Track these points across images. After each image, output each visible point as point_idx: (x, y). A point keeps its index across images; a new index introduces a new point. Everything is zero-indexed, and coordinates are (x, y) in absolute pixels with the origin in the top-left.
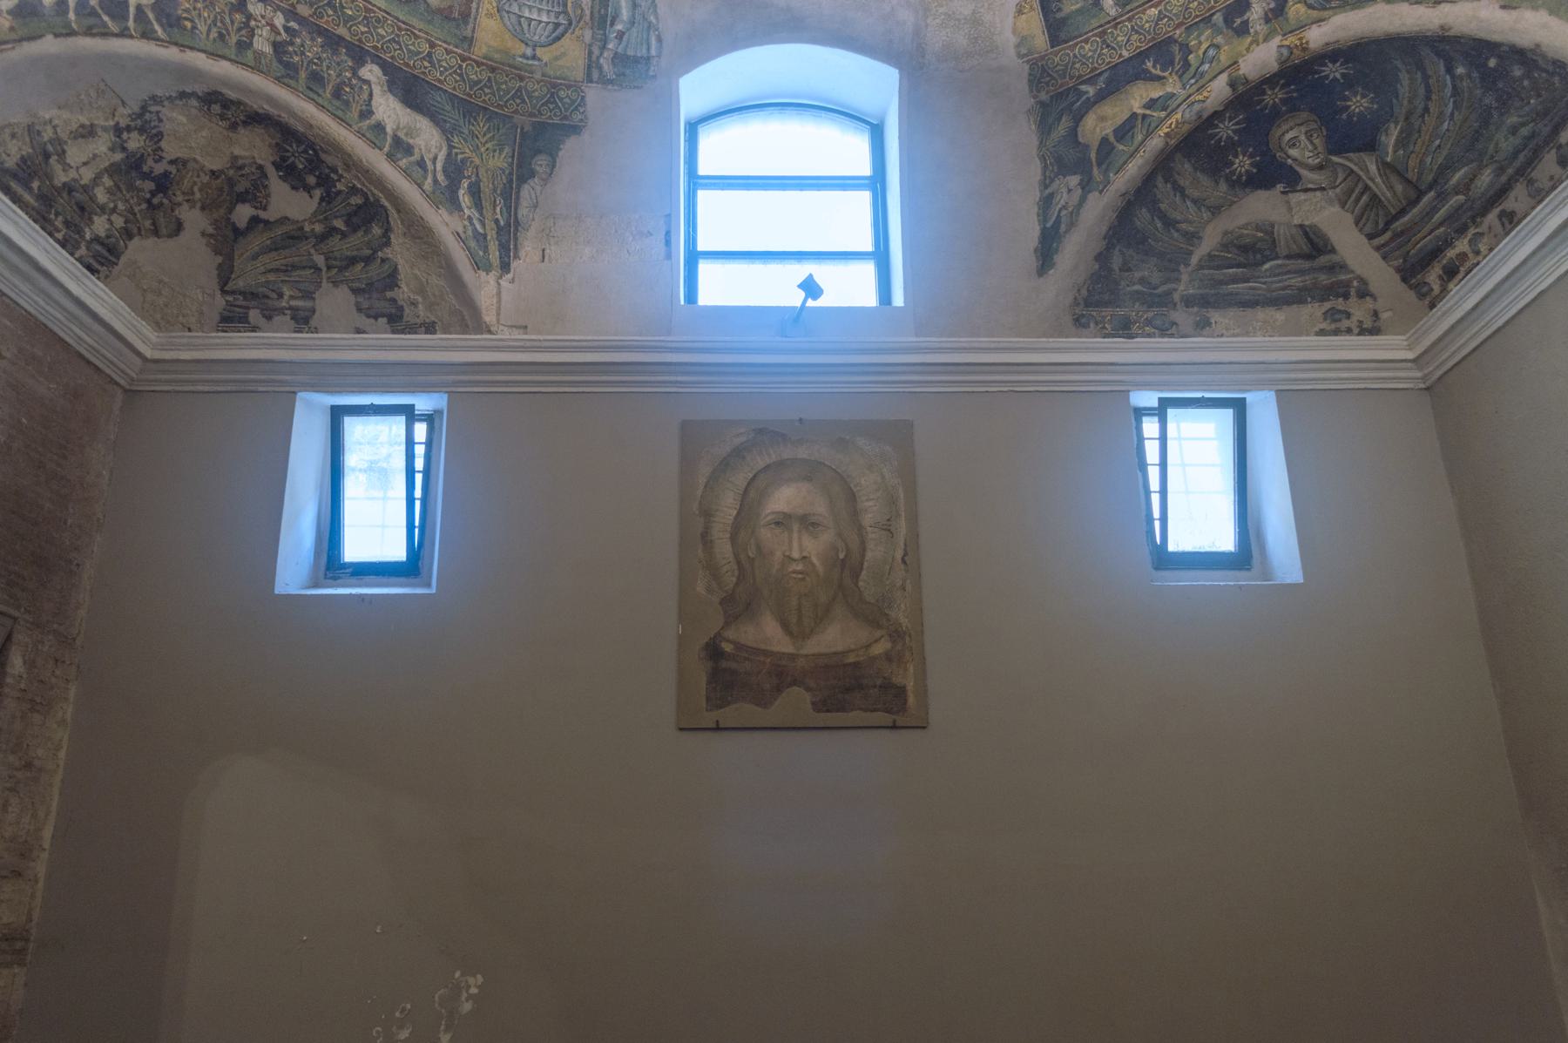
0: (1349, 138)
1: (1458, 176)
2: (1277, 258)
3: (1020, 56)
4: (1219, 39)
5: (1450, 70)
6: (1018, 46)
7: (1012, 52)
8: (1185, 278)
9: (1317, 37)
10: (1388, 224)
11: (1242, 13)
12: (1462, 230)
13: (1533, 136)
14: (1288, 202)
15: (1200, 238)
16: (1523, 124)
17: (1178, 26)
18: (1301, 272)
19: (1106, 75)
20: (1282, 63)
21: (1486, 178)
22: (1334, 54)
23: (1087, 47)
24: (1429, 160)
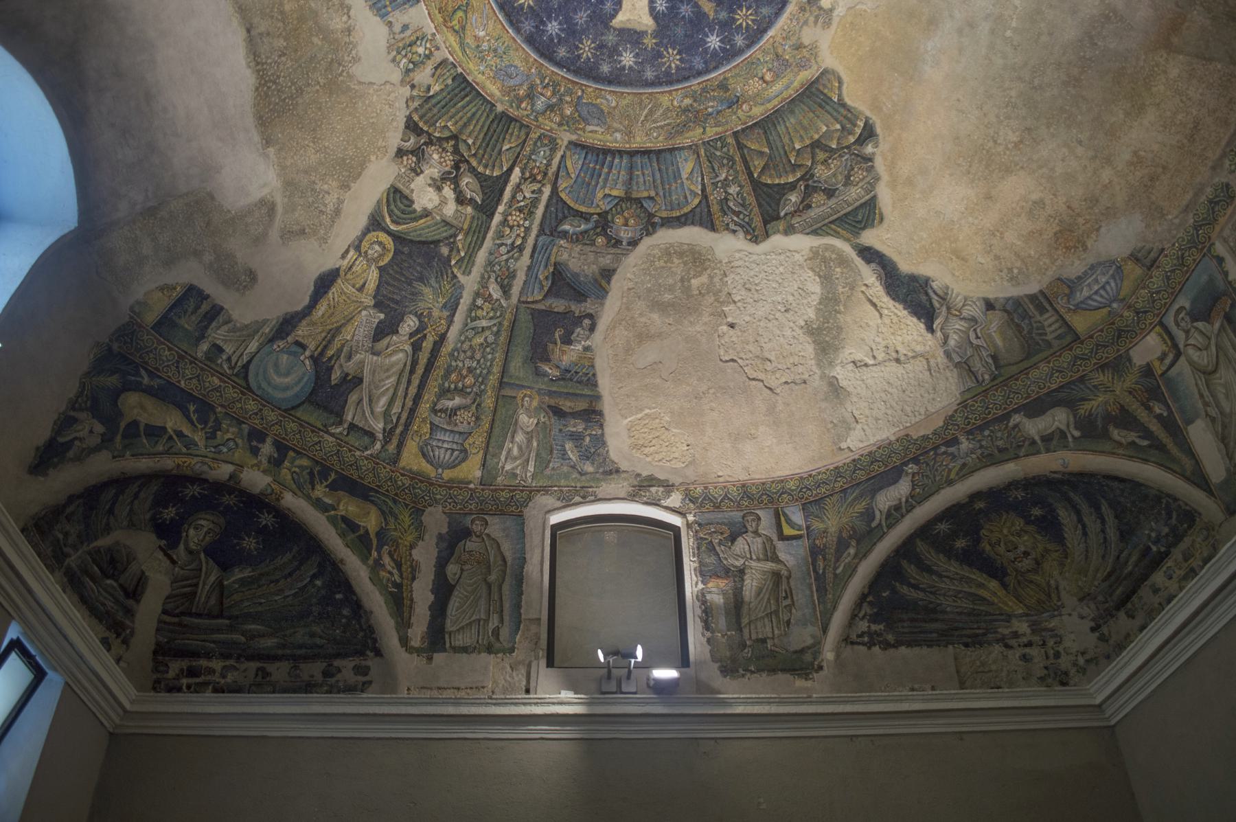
4: (239, 441)
5: (314, 577)
9: (290, 500)
11: (259, 442)
13: (321, 647)
20: (261, 493)
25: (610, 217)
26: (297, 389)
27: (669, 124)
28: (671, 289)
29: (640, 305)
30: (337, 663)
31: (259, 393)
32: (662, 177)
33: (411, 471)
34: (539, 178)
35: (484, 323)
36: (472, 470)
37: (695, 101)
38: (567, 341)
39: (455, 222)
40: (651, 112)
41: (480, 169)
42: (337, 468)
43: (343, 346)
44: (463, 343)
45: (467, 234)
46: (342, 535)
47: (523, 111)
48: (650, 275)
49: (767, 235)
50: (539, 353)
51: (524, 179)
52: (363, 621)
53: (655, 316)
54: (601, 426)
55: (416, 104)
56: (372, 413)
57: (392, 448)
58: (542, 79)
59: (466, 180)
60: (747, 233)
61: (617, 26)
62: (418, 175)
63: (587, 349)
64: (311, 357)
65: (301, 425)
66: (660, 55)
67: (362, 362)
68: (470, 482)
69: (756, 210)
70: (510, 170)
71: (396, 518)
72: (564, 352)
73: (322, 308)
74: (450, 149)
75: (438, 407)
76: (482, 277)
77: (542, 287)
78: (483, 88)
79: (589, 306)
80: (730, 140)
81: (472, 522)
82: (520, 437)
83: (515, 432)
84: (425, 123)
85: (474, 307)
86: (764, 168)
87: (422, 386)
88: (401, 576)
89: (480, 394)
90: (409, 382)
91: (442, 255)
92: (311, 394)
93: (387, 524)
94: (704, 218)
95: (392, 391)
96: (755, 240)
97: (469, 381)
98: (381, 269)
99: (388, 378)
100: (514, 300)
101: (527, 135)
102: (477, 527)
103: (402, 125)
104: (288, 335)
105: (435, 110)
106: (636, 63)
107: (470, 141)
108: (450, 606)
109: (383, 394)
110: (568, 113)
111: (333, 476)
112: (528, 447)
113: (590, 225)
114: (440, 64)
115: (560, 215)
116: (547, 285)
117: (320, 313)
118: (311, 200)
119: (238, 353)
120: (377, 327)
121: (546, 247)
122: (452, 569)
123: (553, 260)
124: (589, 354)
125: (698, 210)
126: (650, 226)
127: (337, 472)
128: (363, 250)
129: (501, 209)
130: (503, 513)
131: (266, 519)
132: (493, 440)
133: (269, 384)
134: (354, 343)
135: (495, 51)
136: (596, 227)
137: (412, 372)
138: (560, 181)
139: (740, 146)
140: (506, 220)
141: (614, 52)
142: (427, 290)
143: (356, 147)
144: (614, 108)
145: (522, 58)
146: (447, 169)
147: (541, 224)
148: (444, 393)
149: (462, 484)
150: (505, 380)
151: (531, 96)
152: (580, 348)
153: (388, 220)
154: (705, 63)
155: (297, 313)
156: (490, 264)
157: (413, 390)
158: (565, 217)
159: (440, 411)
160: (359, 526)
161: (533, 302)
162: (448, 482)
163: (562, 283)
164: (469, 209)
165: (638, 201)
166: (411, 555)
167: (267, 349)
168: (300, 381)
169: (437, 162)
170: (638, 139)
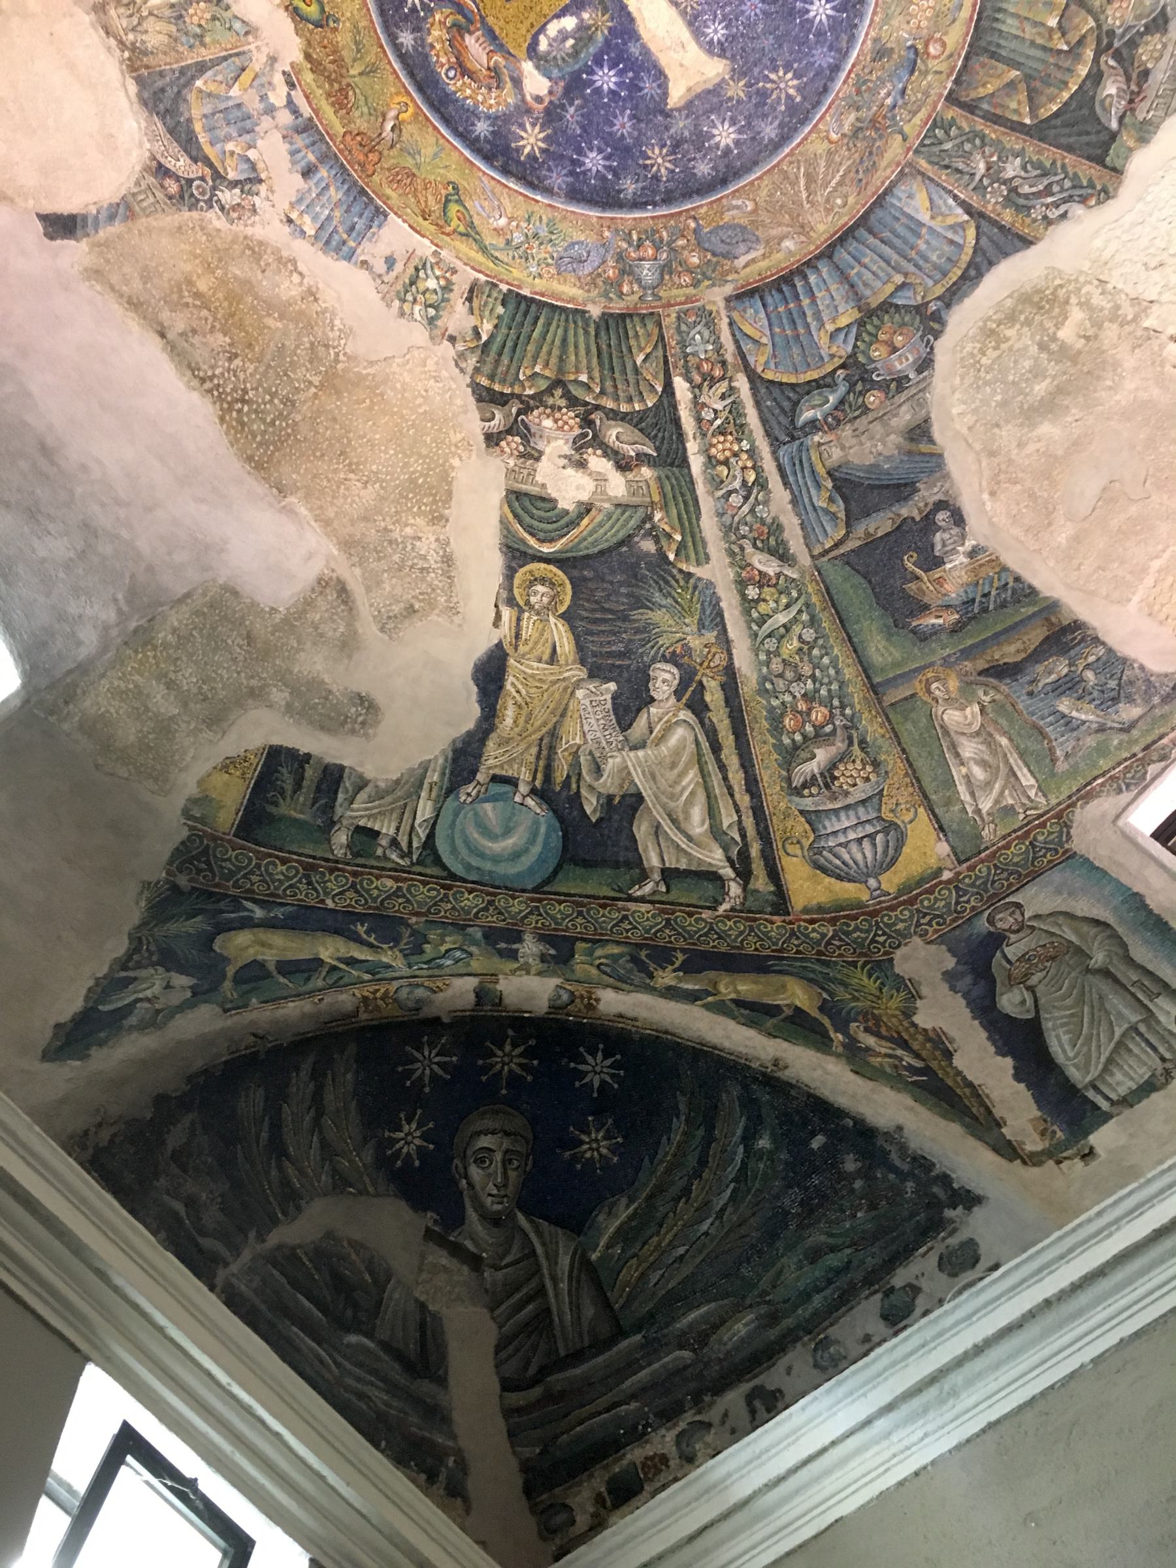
0: (557, 1194)
1: (692, 1316)
2: (370, 1335)
3: (186, 813)
5: (748, 1138)
6: (194, 801)
7: (180, 802)
8: (246, 1256)
9: (613, 1001)
10: (544, 1371)
12: (668, 1416)
14: (423, 1256)
15: (299, 1209)
16: (833, 1249)
17: (417, 914)
18: (392, 1388)
19: (290, 909)
20: (554, 1008)
21: (741, 1327)
22: (618, 1040)
23: (280, 868)
24: (654, 1277)
25: (861, 359)
26: (536, 849)
27: (848, 171)
28: (1037, 373)
29: (1007, 435)
30: (900, 1278)
31: (471, 878)
32: (893, 247)
33: (820, 909)
34: (717, 373)
35: (782, 618)
36: (926, 850)
37: (858, 109)
38: (933, 562)
39: (636, 500)
40: (810, 178)
41: (624, 408)
42: (682, 944)
43: (575, 755)
44: (768, 663)
45: (665, 507)
46: (750, 1023)
47: (630, 297)
48: (986, 383)
49: (1118, 172)
50: (901, 609)
51: (696, 388)
52: (894, 1157)
53: (1046, 429)
54: (1097, 641)
55: (472, 361)
56: (690, 838)
57: (761, 882)
58: (628, 238)
59: (613, 433)
60: (1083, 200)
61: (682, 103)
62: (538, 459)
63: (973, 553)
64: (533, 792)
65: (582, 905)
66: (763, 95)
67: (625, 772)
68: (939, 871)
69: (1070, 159)
70: (668, 387)
71: (846, 985)
72: (940, 581)
73: (508, 716)
74: (562, 403)
75: (797, 782)
76: (732, 554)
77: (834, 517)
78: (553, 295)
79: (928, 494)
80: (952, 113)
81: (991, 920)
82: (969, 749)
83: (954, 747)
84: (503, 382)
85: (748, 605)
86: (1031, 99)
87: (746, 764)
88: (918, 1056)
89: (852, 724)
90: (722, 768)
91: (647, 554)
92: (565, 848)
93: (831, 994)
94: (1001, 241)
95: (701, 797)
96: (1106, 195)
97: (819, 714)
98: (566, 617)
99: (682, 775)
100: (805, 560)
101: (660, 325)
102: (1005, 921)
103: (471, 400)
104: (474, 772)
105: (505, 360)
106: (740, 131)
107: (584, 378)
108: (1055, 1048)
109: (690, 802)
110: (695, 260)
111: (681, 957)
112: (994, 753)
113: (842, 389)
114: (471, 291)
115: (786, 405)
116: (839, 508)
117: (509, 721)
118: (396, 558)
119: (405, 827)
120: (614, 704)
121: (799, 462)
122: (1010, 1002)
123: (821, 471)
124: (982, 558)
125: (984, 241)
126: (931, 322)
127: (683, 951)
128: (521, 603)
129: (692, 447)
130: (1034, 875)
131: (597, 1070)
132: (926, 783)
133: (482, 856)
134: (591, 745)
135: (536, 236)
136: (852, 386)
137: (716, 748)
138: (751, 360)
139: (971, 108)
140: (710, 458)
141: (700, 140)
142: (658, 616)
143: (420, 455)
144: (755, 211)
145: (581, 225)
146: (577, 431)
147: (768, 434)
148: (791, 756)
149: (928, 881)
150: (877, 680)
151: (627, 270)
152: (960, 559)
153: (532, 541)
154: (831, 48)
155: (469, 734)
156: (729, 530)
157: (737, 777)
158: (796, 404)
159: (805, 785)
160: (778, 1006)
161: (836, 546)
162: (901, 891)
163: (857, 492)
164: (646, 472)
165: (887, 307)
166: (915, 1025)
167: (450, 803)
168: (534, 835)
169: (555, 435)
170: (821, 228)
